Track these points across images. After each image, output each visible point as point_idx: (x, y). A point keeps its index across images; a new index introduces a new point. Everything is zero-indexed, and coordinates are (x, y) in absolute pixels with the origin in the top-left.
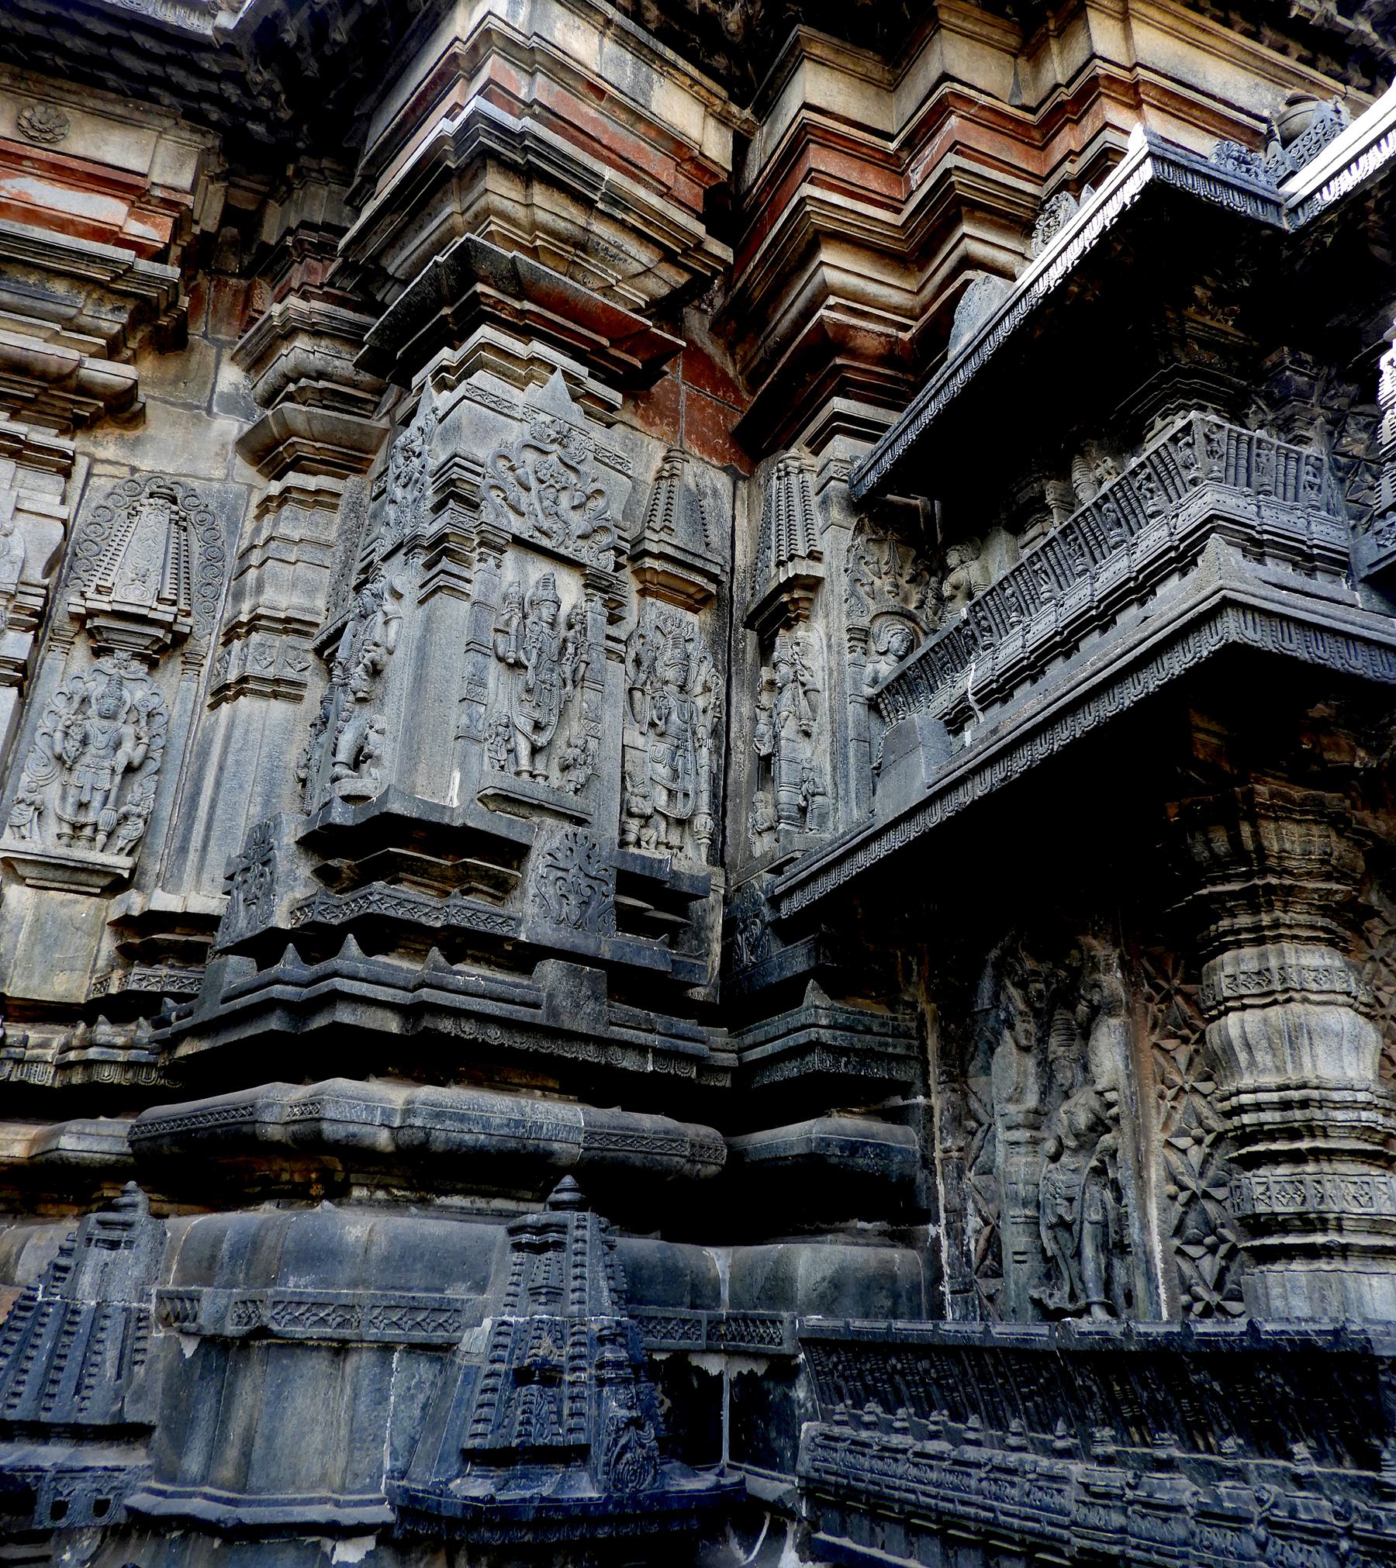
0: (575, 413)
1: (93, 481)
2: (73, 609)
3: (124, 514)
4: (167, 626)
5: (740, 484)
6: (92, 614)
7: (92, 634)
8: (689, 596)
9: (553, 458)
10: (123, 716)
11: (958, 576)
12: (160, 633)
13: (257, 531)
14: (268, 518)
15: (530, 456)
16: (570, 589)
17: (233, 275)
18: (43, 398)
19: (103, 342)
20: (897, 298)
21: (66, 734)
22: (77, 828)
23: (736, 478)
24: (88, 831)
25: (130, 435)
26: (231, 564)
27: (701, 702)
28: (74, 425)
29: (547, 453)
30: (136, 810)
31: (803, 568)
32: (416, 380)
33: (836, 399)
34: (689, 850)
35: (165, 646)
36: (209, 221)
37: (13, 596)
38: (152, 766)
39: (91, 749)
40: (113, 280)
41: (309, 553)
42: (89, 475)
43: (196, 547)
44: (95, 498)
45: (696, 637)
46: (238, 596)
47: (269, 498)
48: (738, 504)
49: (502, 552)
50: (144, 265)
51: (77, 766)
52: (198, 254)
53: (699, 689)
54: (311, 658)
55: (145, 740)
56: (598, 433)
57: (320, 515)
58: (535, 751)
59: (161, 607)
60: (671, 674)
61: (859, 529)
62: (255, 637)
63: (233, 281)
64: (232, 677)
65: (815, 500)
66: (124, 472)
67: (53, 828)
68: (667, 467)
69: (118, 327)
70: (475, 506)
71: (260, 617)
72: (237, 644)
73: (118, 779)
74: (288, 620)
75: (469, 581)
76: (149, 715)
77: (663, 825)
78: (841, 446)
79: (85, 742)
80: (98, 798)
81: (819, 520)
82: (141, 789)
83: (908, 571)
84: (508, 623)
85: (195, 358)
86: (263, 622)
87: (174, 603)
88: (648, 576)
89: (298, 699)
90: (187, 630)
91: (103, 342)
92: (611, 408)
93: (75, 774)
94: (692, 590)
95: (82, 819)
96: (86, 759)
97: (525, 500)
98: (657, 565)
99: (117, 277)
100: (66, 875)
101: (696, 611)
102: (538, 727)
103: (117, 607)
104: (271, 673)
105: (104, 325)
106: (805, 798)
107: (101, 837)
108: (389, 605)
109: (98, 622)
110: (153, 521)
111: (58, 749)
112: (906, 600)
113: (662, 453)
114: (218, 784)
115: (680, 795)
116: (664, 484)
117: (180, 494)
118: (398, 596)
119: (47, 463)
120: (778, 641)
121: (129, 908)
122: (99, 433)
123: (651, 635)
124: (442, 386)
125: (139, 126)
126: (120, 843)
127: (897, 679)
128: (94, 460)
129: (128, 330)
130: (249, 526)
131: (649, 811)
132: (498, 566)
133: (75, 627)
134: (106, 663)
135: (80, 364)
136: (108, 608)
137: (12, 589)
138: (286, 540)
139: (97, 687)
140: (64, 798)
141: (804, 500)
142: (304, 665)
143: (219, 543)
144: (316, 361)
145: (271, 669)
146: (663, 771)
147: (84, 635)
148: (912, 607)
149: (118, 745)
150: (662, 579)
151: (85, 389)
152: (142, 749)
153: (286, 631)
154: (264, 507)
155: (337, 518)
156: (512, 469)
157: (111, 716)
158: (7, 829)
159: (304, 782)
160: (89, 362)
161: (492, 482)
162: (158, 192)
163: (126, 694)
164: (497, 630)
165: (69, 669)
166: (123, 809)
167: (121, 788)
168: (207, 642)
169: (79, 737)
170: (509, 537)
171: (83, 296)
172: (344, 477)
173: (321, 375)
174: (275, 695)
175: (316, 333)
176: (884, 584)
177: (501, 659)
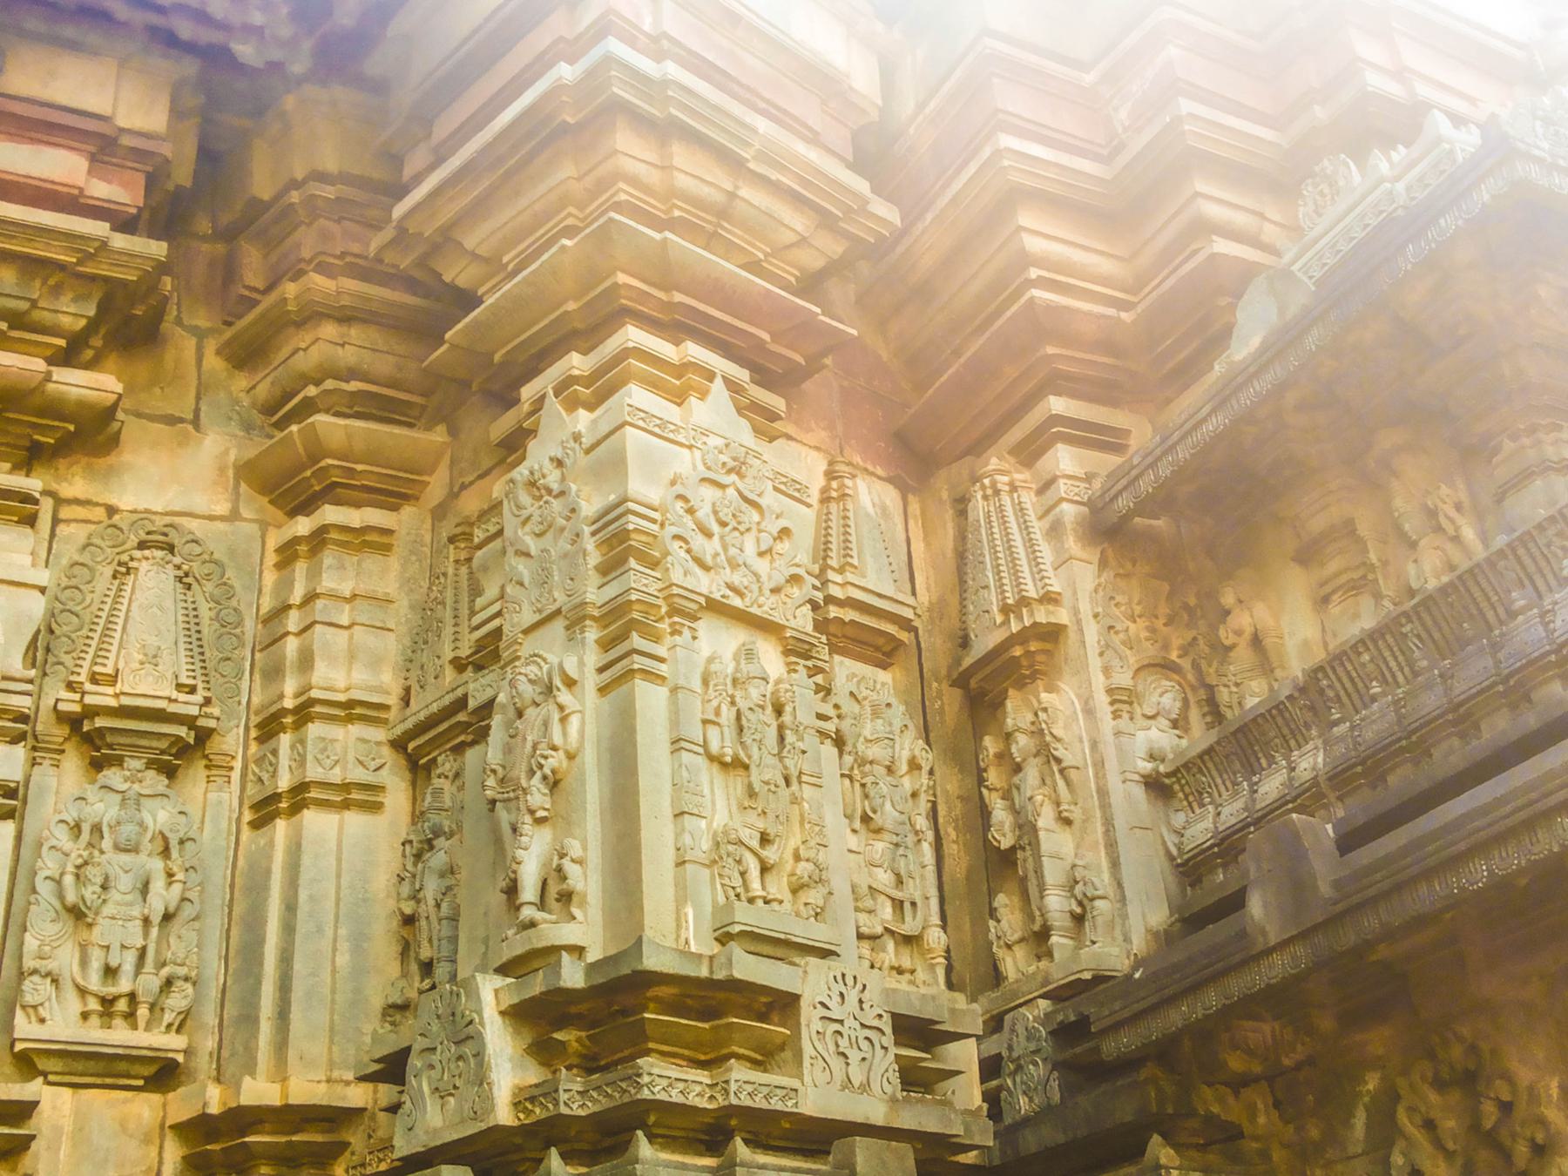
0: (743, 433)
1: (62, 530)
2: (62, 707)
3: (108, 571)
4: (188, 721)
5: (911, 497)
6: (91, 712)
8: (877, 649)
9: (731, 491)
10: (146, 845)
11: (1243, 620)
12: (182, 731)
13: (286, 584)
14: (301, 567)
15: (709, 493)
16: (771, 659)
17: (204, 238)
19: (62, 342)
20: (1106, 266)
21: (77, 876)
22: (107, 1002)
23: (904, 490)
24: (122, 1005)
25: (102, 462)
26: (250, 627)
27: (907, 784)
29: (722, 487)
30: (182, 971)
31: (1042, 615)
32: (527, 392)
33: (1052, 399)
34: (921, 975)
35: (182, 749)
36: (183, 175)
38: (188, 911)
39: (114, 895)
40: (80, 262)
41: (365, 612)
42: (56, 521)
43: (205, 612)
44: (67, 551)
45: (893, 700)
46: (274, 673)
47: (296, 540)
48: (911, 523)
49: (695, 619)
50: (120, 241)
51: (100, 920)
52: (165, 214)
53: (904, 768)
54: (387, 753)
55: (180, 876)
56: (767, 450)
57: (372, 562)
58: (765, 869)
59: (182, 697)
60: (873, 752)
61: (1103, 564)
62: (314, 729)
63: (205, 247)
64: (284, 783)
65: (1038, 528)
66: (100, 513)
67: (74, 1005)
68: (834, 484)
69: (83, 323)
70: (654, 564)
71: (313, 702)
72: (285, 740)
73: (154, 931)
74: (350, 704)
75: (662, 660)
76: (182, 842)
77: (890, 945)
78: (1065, 459)
79: (104, 887)
80: (129, 960)
81: (1046, 553)
82: (180, 943)
83: (1163, 610)
84: (717, 712)
85: (170, 356)
86: (318, 709)
87: (192, 690)
88: (832, 629)
89: (375, 807)
90: (212, 724)
91: (62, 342)
92: (773, 416)
93: (96, 930)
94: (881, 641)
95: (111, 990)
96: (108, 910)
97: (708, 548)
98: (849, 615)
99: (88, 257)
100: (100, 1066)
101: (884, 666)
102: (765, 840)
103: (126, 701)
104: (336, 776)
105: (65, 321)
106: (1080, 903)
107: (143, 1012)
108: (564, 697)
109: (100, 722)
110: (153, 581)
111: (71, 898)
112: (1166, 647)
113: (823, 466)
114: (289, 929)
115: (907, 906)
116: (833, 507)
117: (175, 538)
118: (570, 683)
120: (1009, 704)
121: (205, 1105)
122: (62, 463)
123: (849, 707)
124: (572, 404)
125: (95, 53)
126: (168, 1017)
127: (1201, 756)
128: (59, 502)
129: (93, 325)
130: (270, 578)
131: (879, 930)
132: (694, 638)
133: (65, 730)
134: (112, 776)
135: (48, 378)
136: (113, 703)
138: (334, 596)
139: (103, 808)
140: (84, 963)
141: (1025, 527)
142: (379, 762)
143: (234, 603)
144: (348, 356)
145: (337, 770)
146: (884, 878)
148: (1174, 656)
149: (145, 890)
150: (850, 631)
151: (55, 409)
152: (177, 889)
153: (350, 719)
154: (288, 553)
155: (394, 562)
156: (691, 511)
157: (134, 849)
158: (19, 1013)
159: (409, 920)
160: (59, 374)
161: (674, 530)
162: (126, 141)
163: (149, 820)
164: (705, 722)
165: (62, 787)
166: (165, 971)
167: (158, 943)
168: (233, 740)
169: (99, 880)
170: (702, 601)
171: (37, 283)
172: (394, 508)
173: (352, 374)
174: (346, 805)
175: (345, 317)
176: (1137, 629)
177: (712, 758)
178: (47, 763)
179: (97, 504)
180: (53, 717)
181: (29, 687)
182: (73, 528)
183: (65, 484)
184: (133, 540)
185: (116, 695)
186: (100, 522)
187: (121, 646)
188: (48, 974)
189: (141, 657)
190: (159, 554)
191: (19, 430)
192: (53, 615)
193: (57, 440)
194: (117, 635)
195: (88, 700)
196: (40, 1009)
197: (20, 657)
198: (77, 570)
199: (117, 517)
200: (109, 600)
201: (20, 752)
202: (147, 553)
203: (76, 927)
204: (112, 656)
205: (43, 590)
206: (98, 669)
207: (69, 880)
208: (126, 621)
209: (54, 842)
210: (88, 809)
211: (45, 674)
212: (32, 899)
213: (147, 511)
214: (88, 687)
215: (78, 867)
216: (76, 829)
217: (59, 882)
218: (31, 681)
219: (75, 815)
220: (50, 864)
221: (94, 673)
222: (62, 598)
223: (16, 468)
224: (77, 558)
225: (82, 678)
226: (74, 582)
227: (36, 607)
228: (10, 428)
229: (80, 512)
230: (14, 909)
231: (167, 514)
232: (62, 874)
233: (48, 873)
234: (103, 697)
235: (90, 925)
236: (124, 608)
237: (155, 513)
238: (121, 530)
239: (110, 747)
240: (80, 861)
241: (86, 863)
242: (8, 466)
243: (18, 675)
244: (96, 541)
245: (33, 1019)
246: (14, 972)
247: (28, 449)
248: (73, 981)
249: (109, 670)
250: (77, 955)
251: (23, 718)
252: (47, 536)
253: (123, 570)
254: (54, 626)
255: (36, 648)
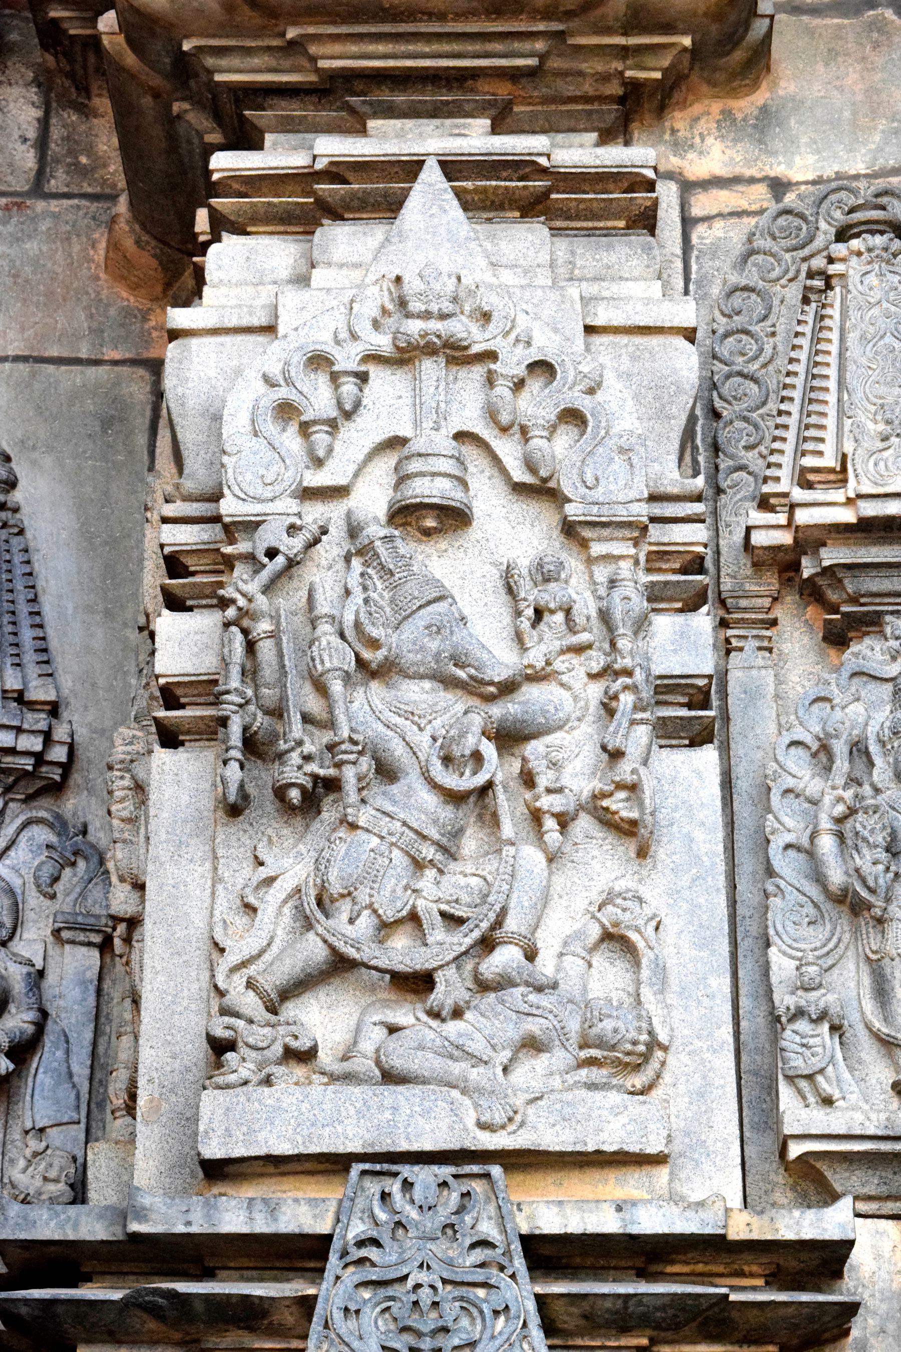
2: (759, 539)
3: (794, 293)
6: (809, 540)
7: (812, 592)
18: (555, 63)
21: (841, 837)
25: (746, 106)
28: (632, 109)
37: (645, 529)
42: (688, 223)
66: (759, 194)
103: (870, 509)
109: (831, 556)
111: (836, 877)
119: (606, 211)
122: (679, 120)
133: (771, 582)
134: (868, 651)
136: (848, 516)
137: (641, 511)
147: (790, 599)
169: (880, 838)
178: (750, 645)
179: (752, 181)
180: (745, 561)
181: (698, 508)
182: (719, 229)
183: (691, 155)
184: (826, 230)
185: (850, 502)
186: (761, 212)
187: (841, 413)
188: (823, 1016)
189: (881, 427)
190: (878, 240)
191: (598, 66)
192: (714, 386)
193: (665, 71)
194: (832, 398)
195: (803, 517)
196: (820, 1078)
197: (674, 457)
198: (737, 301)
199: (790, 199)
200: (805, 342)
201: (703, 621)
202: (855, 243)
203: (856, 931)
204: (830, 435)
205: (690, 335)
206: (809, 461)
207: (827, 844)
208: (842, 369)
209: (790, 782)
210: (838, 714)
211: (719, 491)
212: (771, 888)
213: (839, 176)
214: (799, 494)
215: (839, 820)
216: (822, 754)
217: (811, 853)
218: (699, 498)
219: (817, 729)
220: (789, 822)
221: (804, 470)
222: (724, 351)
223: (606, 137)
224: (734, 279)
225: (783, 487)
226: (738, 321)
227: (685, 364)
228: (584, 66)
229: (724, 199)
230: (741, 910)
231: (875, 175)
232: (813, 837)
233: (789, 838)
234: (828, 509)
235: (880, 921)
236: (834, 348)
237: (856, 177)
238: (801, 216)
239: (854, 600)
240: (840, 809)
241: (852, 812)
242: (594, 136)
243: (675, 490)
244: (761, 243)
245: (812, 1100)
246: (761, 1021)
247: (621, 100)
248: (869, 1027)
249: (829, 461)
250: (866, 980)
251: (696, 565)
252: (679, 252)
253: (818, 283)
254: (718, 404)
255: (695, 448)
